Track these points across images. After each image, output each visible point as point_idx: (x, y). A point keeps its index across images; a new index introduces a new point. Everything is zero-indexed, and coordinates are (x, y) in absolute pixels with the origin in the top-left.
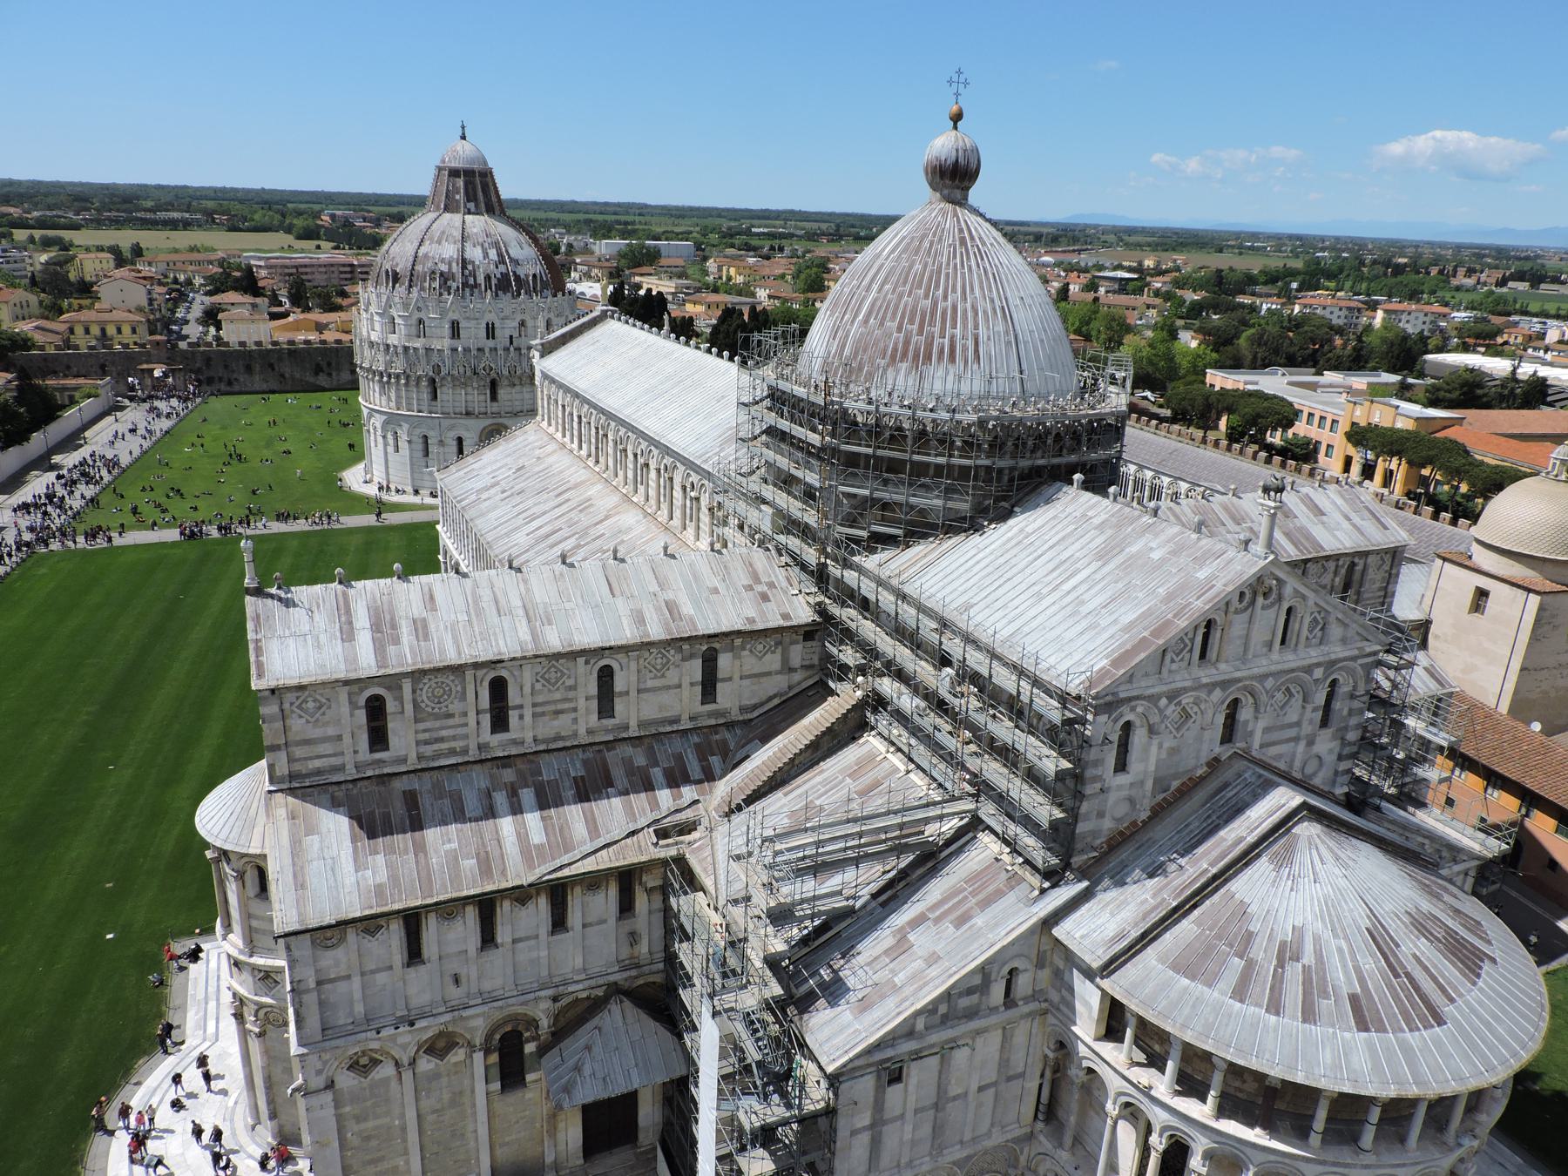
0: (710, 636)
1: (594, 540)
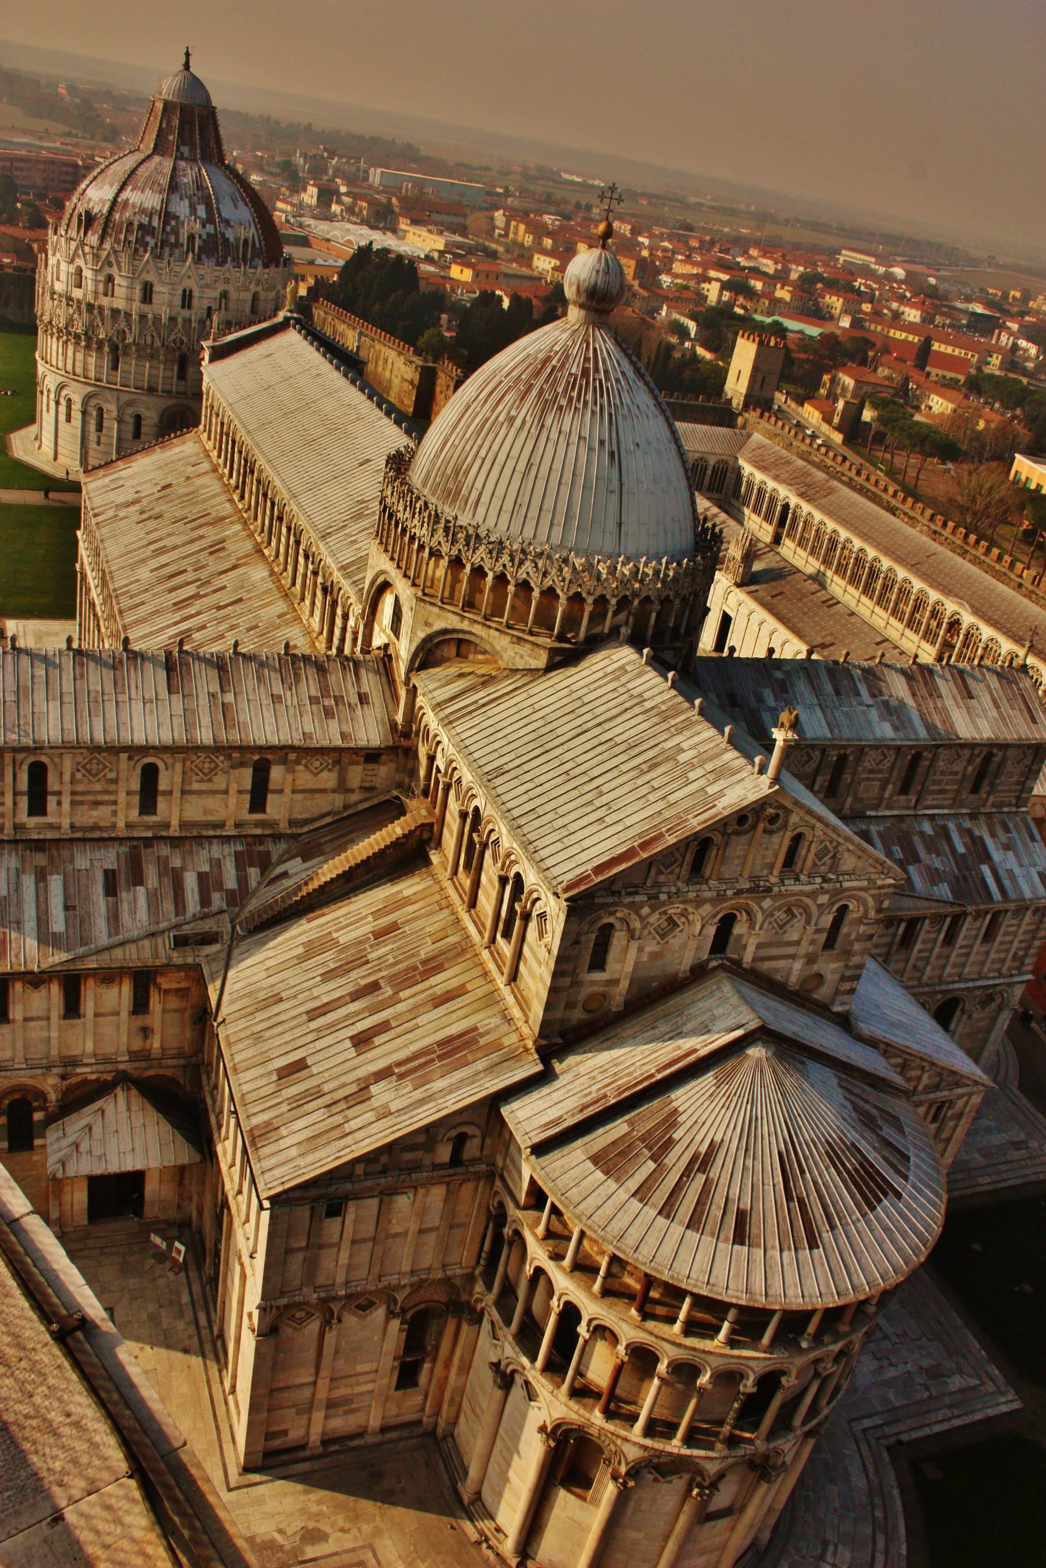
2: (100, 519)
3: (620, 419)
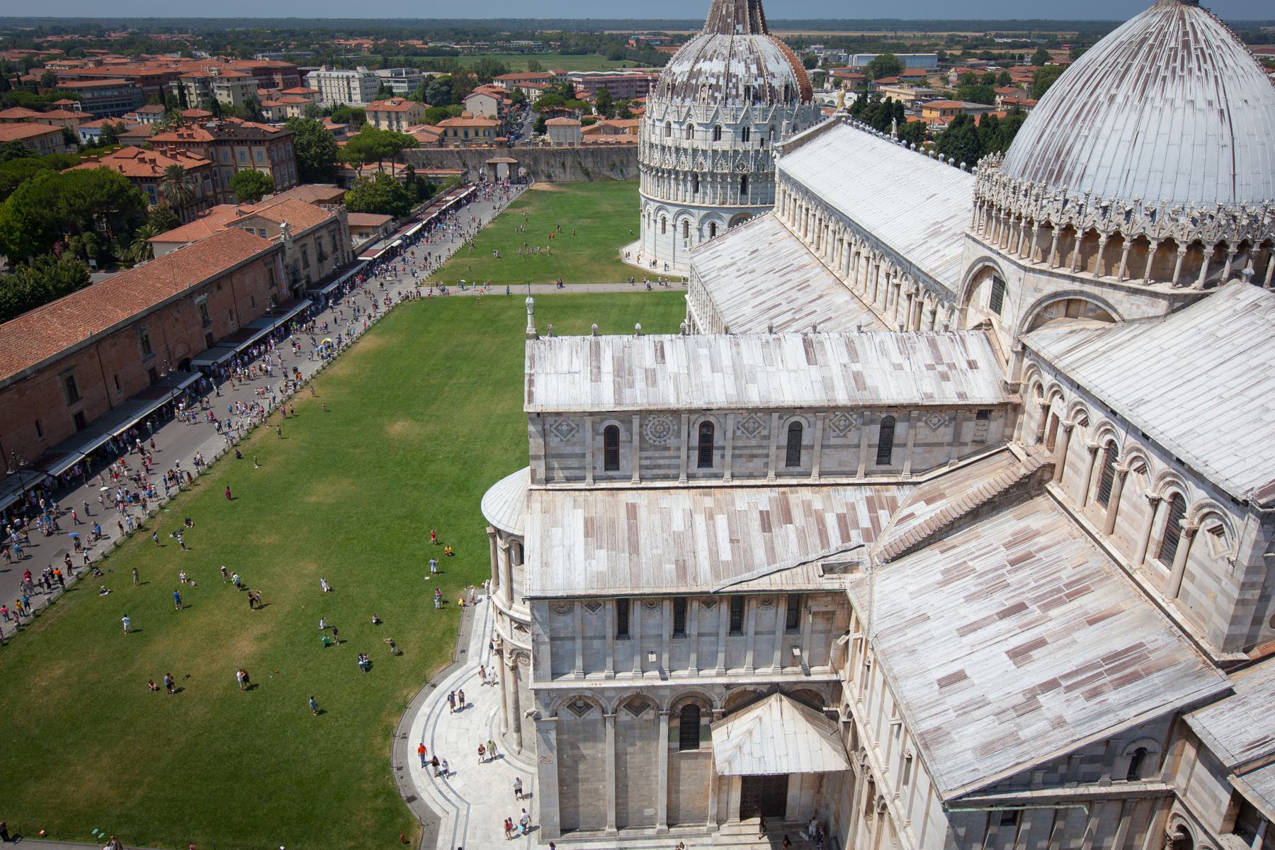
0: (890, 406)
1: (807, 315)
2: (706, 279)
3: (1226, 80)
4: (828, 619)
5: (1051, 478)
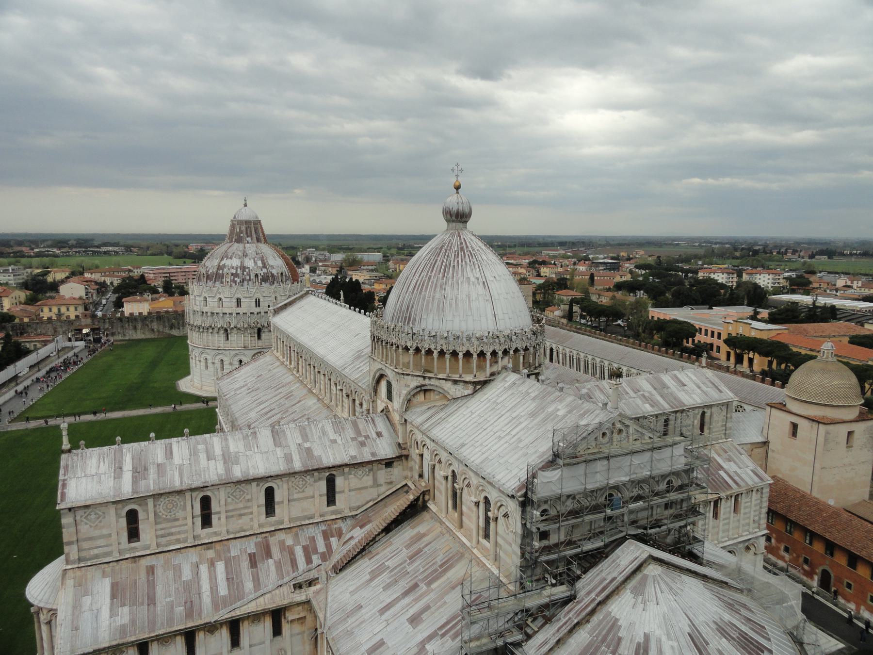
0: (330, 468)
3: (484, 267)
4: (302, 623)
5: (429, 500)
